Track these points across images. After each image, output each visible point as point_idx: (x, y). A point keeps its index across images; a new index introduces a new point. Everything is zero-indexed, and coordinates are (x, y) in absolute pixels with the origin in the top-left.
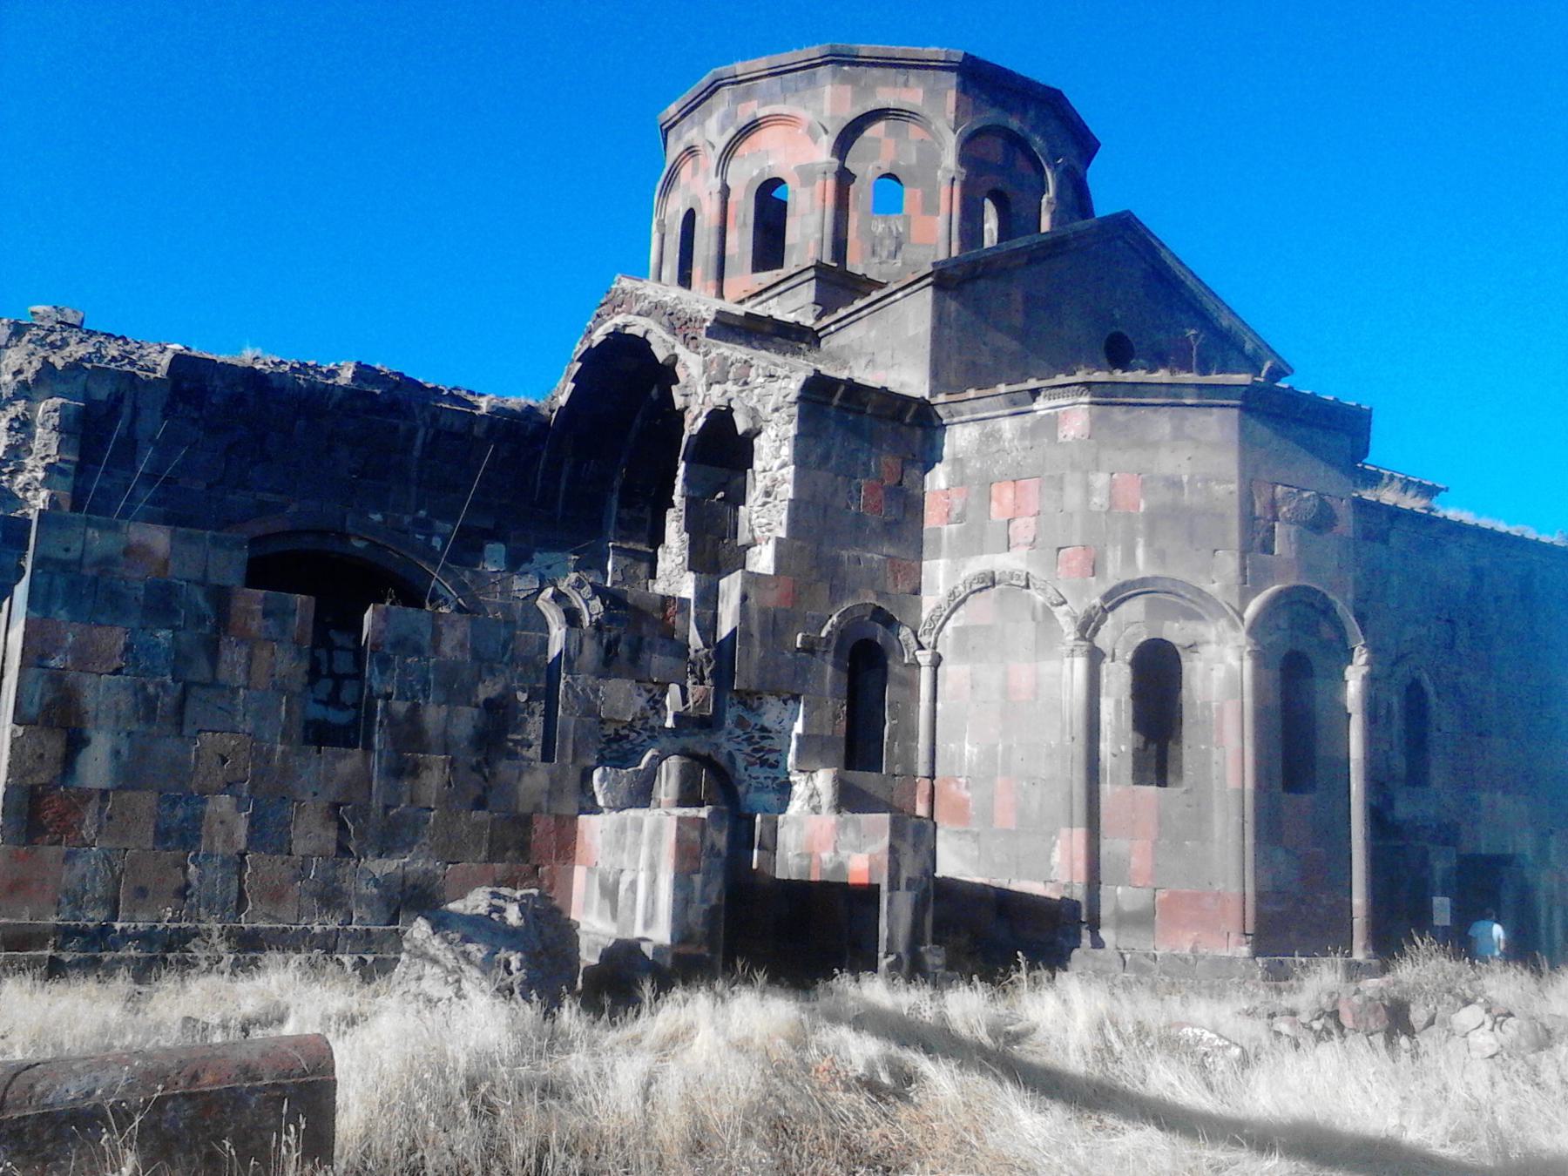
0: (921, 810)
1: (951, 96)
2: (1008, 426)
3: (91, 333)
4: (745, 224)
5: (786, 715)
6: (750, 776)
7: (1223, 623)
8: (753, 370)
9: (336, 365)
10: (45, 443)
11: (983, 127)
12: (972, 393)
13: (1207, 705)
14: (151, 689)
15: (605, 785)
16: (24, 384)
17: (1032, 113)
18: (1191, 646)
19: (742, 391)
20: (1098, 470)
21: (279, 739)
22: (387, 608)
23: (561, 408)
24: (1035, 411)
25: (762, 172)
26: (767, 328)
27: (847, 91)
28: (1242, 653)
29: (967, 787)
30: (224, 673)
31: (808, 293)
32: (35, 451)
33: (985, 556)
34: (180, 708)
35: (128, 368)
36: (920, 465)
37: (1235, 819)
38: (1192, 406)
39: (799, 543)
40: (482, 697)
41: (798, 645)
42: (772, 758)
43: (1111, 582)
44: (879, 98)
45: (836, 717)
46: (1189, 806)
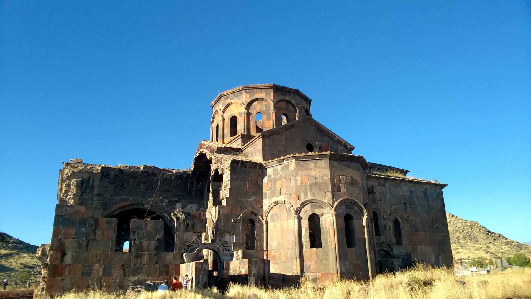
0: (265, 258)
1: (272, 94)
2: (279, 168)
3: (84, 164)
4: (228, 126)
5: (231, 238)
6: (223, 253)
7: (328, 208)
8: (223, 160)
9: (140, 166)
10: (73, 189)
12: (270, 161)
13: (326, 228)
14: (81, 242)
15: (186, 257)
16: (68, 176)
17: (292, 95)
18: (322, 214)
19: (221, 165)
20: (298, 176)
21: (110, 251)
22: (134, 220)
23: (192, 171)
25: (231, 115)
26: (230, 150)
29: (275, 252)
30: (97, 237)
31: (240, 141)
32: (71, 191)
33: (276, 197)
35: (92, 171)
36: (261, 178)
37: (334, 255)
38: (317, 159)
39: (232, 198)
40: (157, 239)
41: (233, 221)
42: (228, 248)
43: (303, 201)
44: (255, 96)
45: (243, 237)
46: (324, 252)
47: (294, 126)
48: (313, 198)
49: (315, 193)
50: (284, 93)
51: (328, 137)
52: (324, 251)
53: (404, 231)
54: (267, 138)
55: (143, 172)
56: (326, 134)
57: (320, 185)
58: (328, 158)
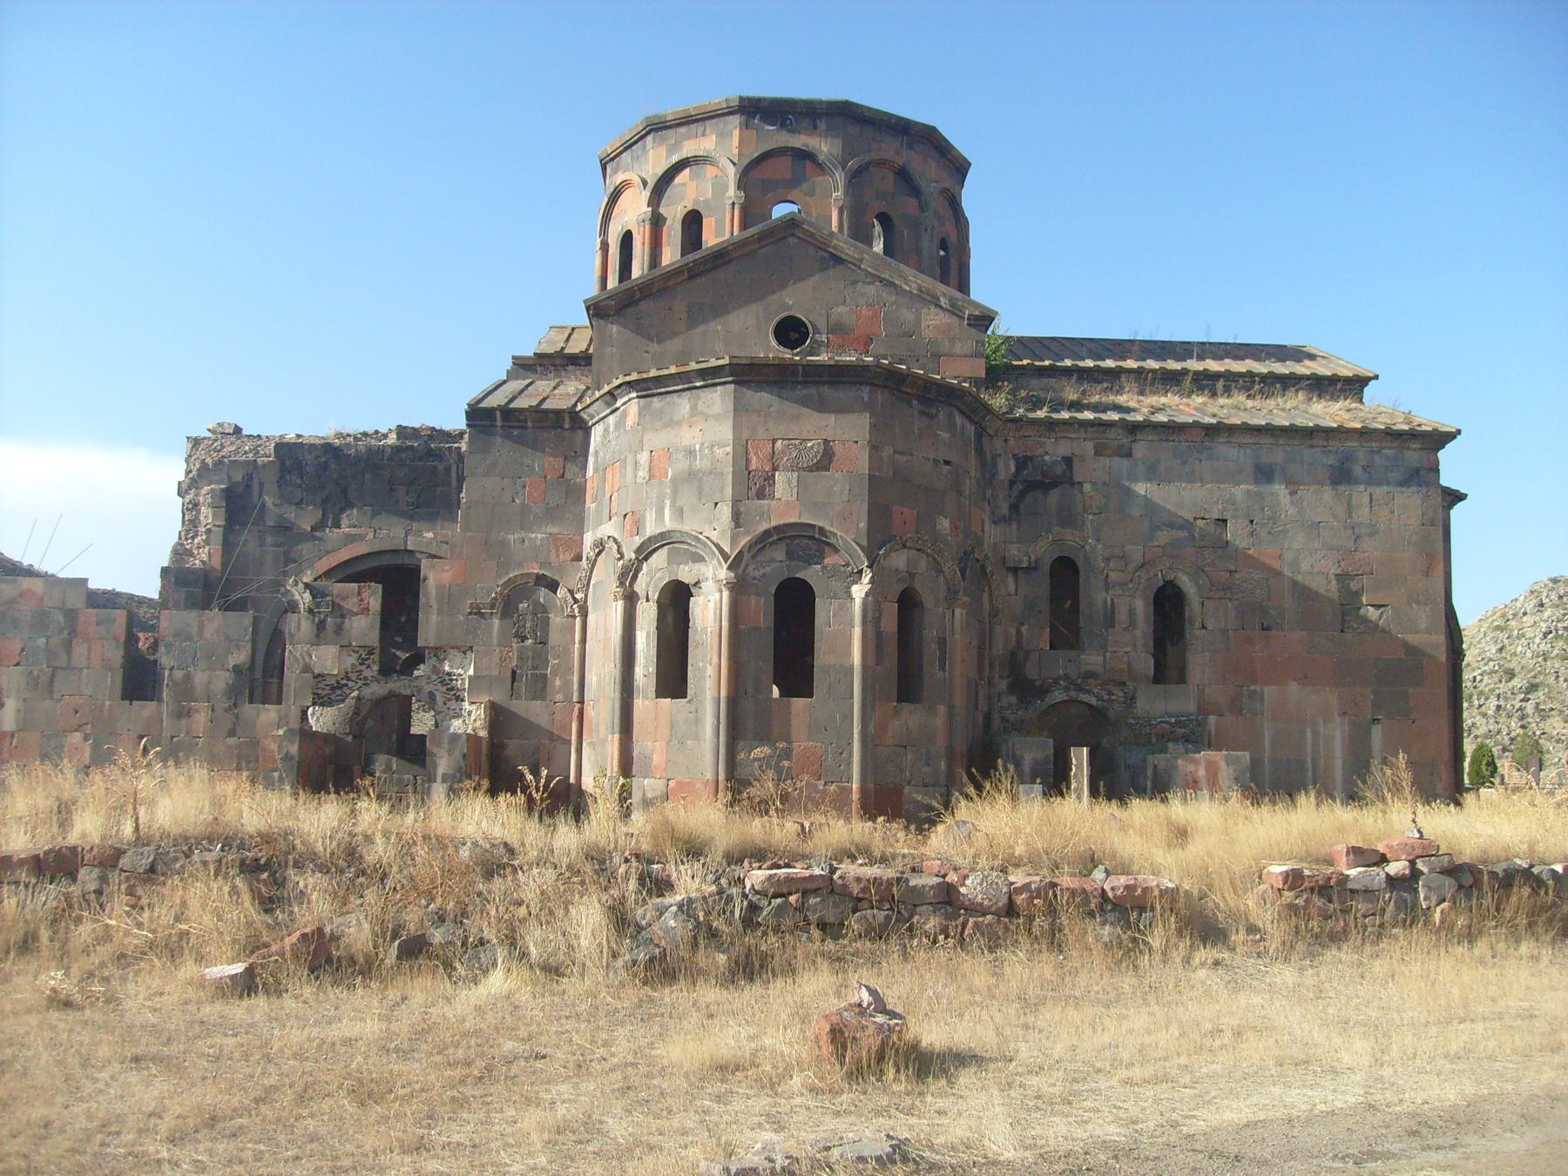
1: (736, 133)
7: (715, 561)
10: (207, 515)
13: (704, 629)
14: (35, 673)
17: (822, 125)
24: (617, 409)
27: (663, 151)
34: (52, 681)
39: (469, 534)
40: (231, 664)
43: (648, 535)
47: (726, 259)
48: (679, 527)
49: (685, 509)
51: (877, 283)
52: (693, 709)
53: (1204, 627)
55: (396, 449)
57: (700, 480)
58: (731, 379)
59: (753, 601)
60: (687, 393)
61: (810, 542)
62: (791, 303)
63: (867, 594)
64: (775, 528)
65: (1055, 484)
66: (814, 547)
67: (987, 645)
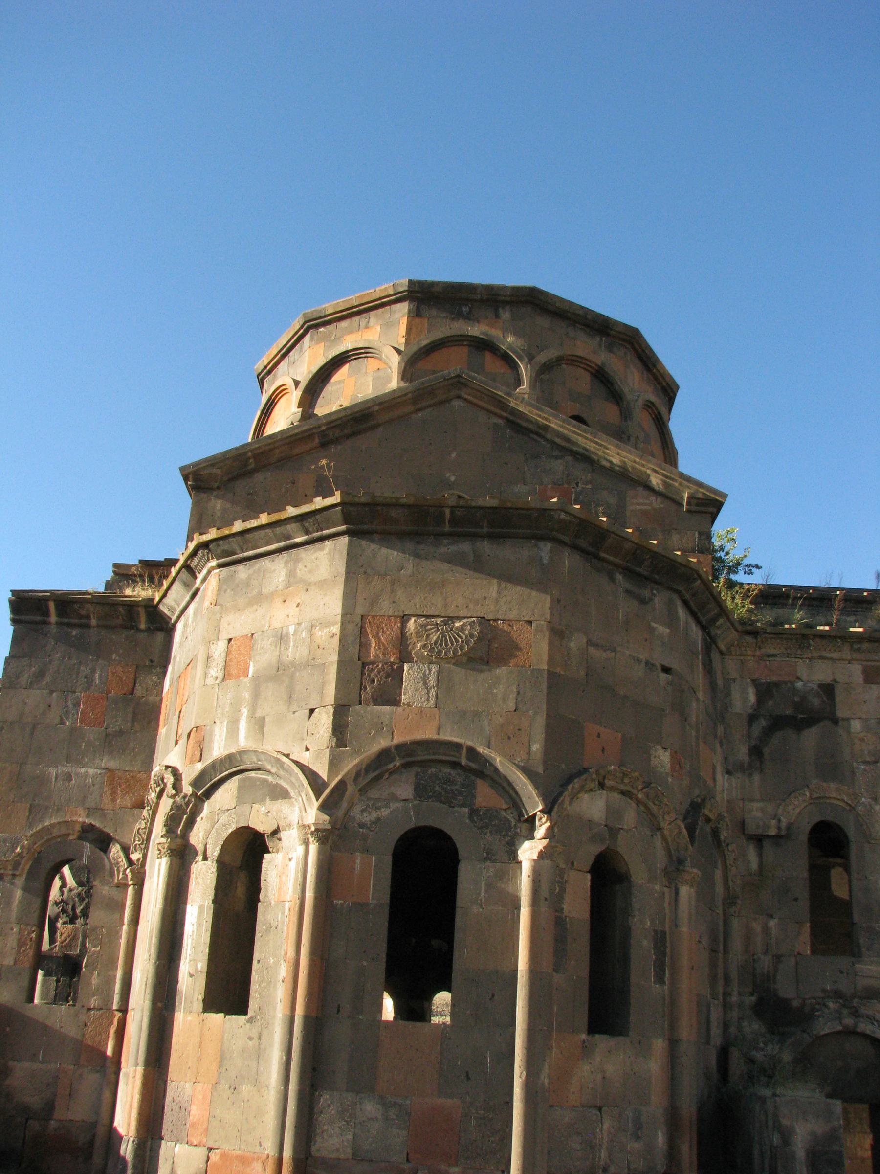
1: (404, 321)
11: (433, 342)
20: (218, 640)
28: (306, 834)
45: (21, 943)
46: (250, 1039)
49: (267, 720)
50: (465, 309)
51: (569, 458)
52: (254, 1033)
54: (218, 488)
56: (557, 440)
57: (292, 677)
58: (343, 528)
59: (358, 861)
60: (285, 555)
61: (453, 772)
62: (453, 479)
63: (541, 855)
64: (399, 747)
65: (811, 720)
66: (459, 780)
67: (721, 948)
